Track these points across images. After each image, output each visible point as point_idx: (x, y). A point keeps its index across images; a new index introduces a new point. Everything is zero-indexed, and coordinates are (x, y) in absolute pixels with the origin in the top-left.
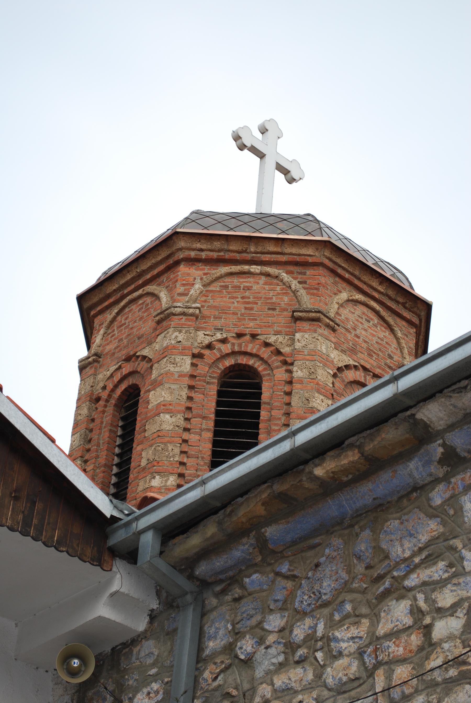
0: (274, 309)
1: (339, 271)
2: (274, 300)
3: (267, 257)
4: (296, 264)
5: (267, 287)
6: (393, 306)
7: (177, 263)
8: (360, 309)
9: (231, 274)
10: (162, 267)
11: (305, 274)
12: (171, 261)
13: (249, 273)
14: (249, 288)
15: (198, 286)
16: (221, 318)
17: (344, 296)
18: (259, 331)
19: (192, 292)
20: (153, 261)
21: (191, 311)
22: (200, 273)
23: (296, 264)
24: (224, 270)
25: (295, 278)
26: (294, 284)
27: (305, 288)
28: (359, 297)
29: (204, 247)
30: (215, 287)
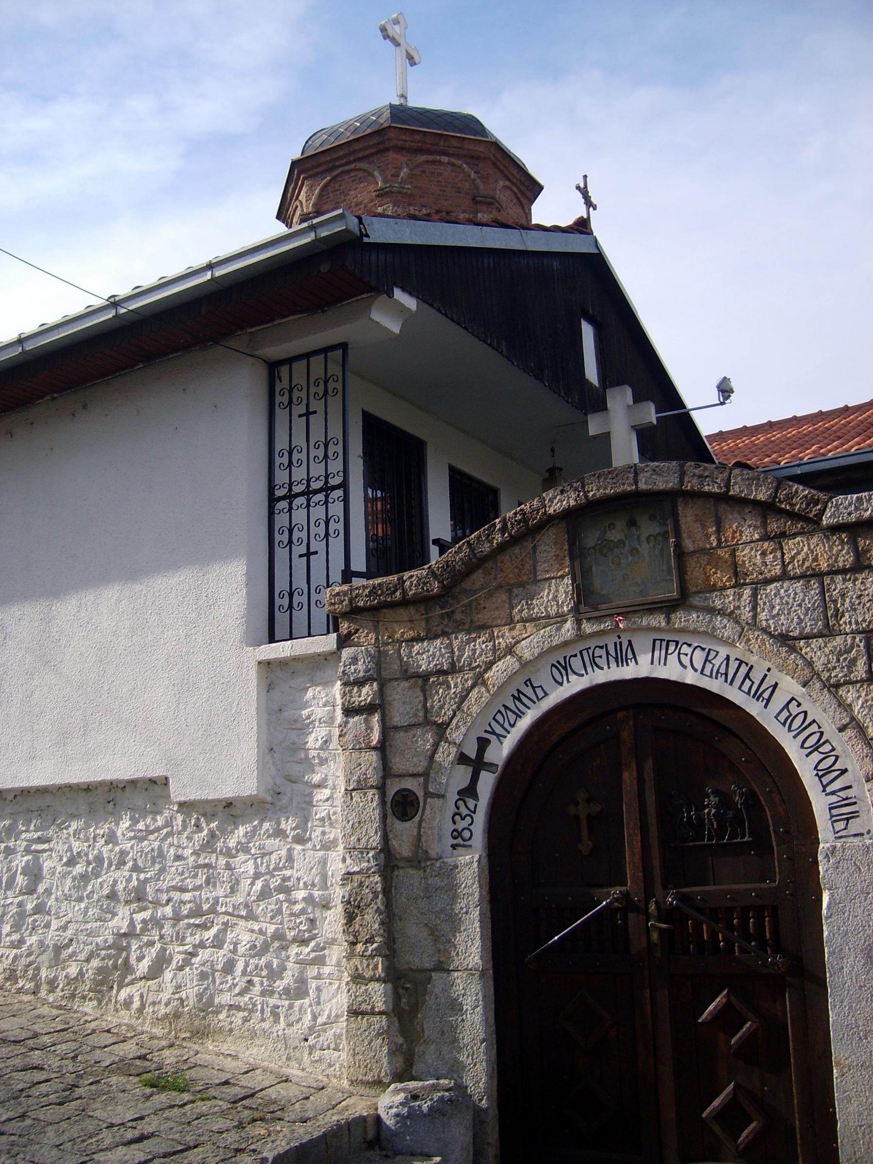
0: (460, 193)
1: (498, 164)
2: (459, 185)
3: (451, 151)
4: (472, 157)
5: (453, 174)
6: (523, 189)
7: (387, 149)
8: (508, 192)
9: (427, 162)
10: (373, 150)
11: (477, 165)
12: (381, 147)
13: (440, 162)
14: (440, 174)
15: (405, 170)
16: (424, 197)
17: (501, 183)
18: (451, 209)
19: (402, 174)
20: (366, 144)
21: (405, 191)
22: (405, 159)
23: (472, 157)
24: (424, 158)
25: (472, 169)
26: (473, 175)
27: (479, 177)
28: (507, 183)
29: (408, 139)
30: (417, 172)
